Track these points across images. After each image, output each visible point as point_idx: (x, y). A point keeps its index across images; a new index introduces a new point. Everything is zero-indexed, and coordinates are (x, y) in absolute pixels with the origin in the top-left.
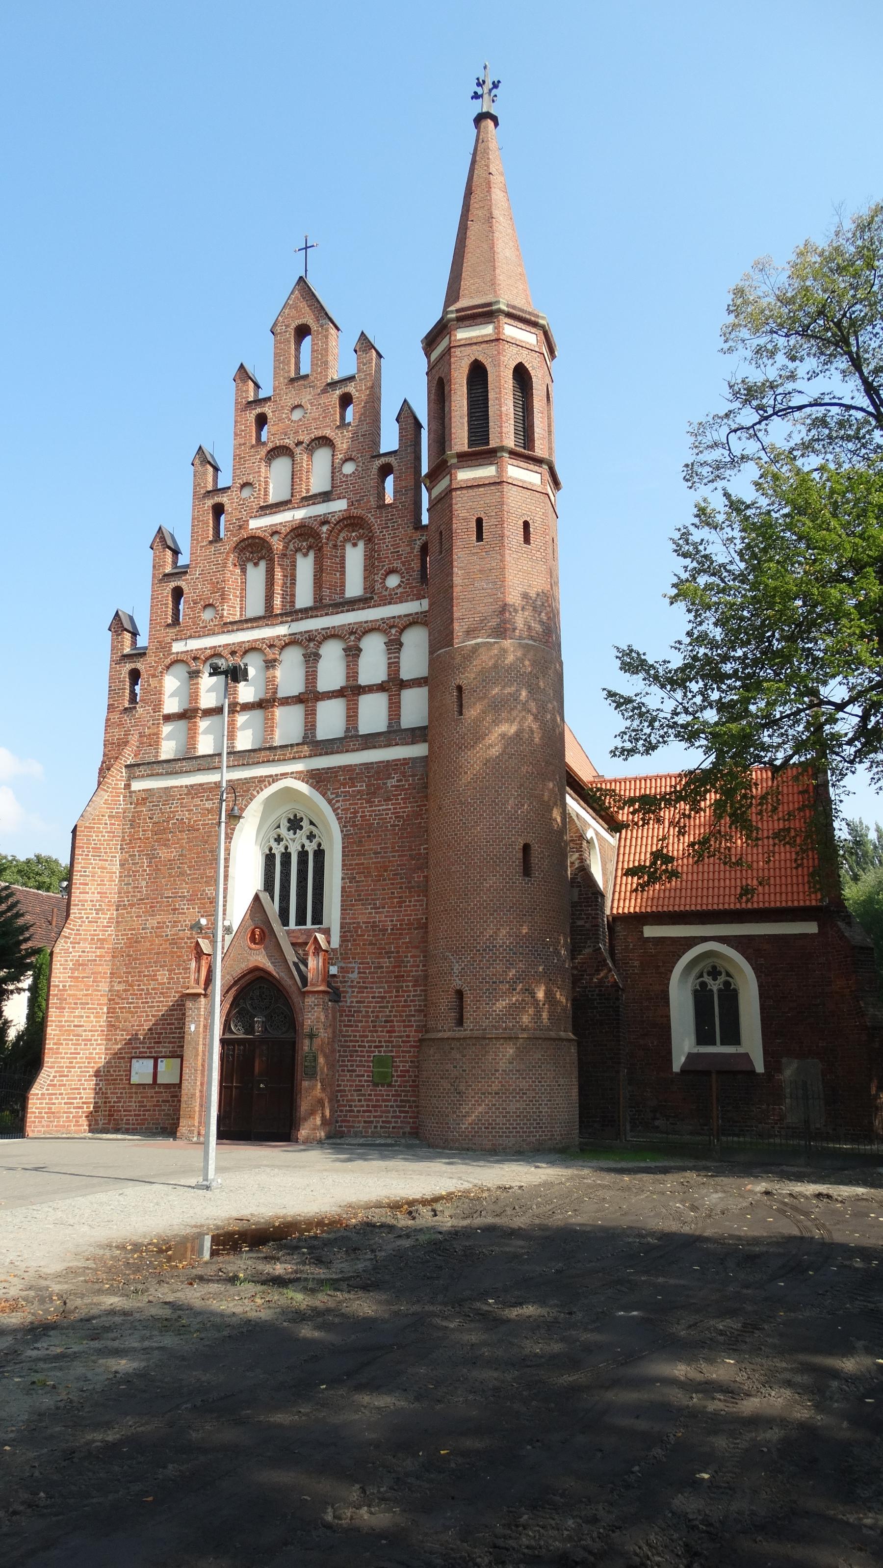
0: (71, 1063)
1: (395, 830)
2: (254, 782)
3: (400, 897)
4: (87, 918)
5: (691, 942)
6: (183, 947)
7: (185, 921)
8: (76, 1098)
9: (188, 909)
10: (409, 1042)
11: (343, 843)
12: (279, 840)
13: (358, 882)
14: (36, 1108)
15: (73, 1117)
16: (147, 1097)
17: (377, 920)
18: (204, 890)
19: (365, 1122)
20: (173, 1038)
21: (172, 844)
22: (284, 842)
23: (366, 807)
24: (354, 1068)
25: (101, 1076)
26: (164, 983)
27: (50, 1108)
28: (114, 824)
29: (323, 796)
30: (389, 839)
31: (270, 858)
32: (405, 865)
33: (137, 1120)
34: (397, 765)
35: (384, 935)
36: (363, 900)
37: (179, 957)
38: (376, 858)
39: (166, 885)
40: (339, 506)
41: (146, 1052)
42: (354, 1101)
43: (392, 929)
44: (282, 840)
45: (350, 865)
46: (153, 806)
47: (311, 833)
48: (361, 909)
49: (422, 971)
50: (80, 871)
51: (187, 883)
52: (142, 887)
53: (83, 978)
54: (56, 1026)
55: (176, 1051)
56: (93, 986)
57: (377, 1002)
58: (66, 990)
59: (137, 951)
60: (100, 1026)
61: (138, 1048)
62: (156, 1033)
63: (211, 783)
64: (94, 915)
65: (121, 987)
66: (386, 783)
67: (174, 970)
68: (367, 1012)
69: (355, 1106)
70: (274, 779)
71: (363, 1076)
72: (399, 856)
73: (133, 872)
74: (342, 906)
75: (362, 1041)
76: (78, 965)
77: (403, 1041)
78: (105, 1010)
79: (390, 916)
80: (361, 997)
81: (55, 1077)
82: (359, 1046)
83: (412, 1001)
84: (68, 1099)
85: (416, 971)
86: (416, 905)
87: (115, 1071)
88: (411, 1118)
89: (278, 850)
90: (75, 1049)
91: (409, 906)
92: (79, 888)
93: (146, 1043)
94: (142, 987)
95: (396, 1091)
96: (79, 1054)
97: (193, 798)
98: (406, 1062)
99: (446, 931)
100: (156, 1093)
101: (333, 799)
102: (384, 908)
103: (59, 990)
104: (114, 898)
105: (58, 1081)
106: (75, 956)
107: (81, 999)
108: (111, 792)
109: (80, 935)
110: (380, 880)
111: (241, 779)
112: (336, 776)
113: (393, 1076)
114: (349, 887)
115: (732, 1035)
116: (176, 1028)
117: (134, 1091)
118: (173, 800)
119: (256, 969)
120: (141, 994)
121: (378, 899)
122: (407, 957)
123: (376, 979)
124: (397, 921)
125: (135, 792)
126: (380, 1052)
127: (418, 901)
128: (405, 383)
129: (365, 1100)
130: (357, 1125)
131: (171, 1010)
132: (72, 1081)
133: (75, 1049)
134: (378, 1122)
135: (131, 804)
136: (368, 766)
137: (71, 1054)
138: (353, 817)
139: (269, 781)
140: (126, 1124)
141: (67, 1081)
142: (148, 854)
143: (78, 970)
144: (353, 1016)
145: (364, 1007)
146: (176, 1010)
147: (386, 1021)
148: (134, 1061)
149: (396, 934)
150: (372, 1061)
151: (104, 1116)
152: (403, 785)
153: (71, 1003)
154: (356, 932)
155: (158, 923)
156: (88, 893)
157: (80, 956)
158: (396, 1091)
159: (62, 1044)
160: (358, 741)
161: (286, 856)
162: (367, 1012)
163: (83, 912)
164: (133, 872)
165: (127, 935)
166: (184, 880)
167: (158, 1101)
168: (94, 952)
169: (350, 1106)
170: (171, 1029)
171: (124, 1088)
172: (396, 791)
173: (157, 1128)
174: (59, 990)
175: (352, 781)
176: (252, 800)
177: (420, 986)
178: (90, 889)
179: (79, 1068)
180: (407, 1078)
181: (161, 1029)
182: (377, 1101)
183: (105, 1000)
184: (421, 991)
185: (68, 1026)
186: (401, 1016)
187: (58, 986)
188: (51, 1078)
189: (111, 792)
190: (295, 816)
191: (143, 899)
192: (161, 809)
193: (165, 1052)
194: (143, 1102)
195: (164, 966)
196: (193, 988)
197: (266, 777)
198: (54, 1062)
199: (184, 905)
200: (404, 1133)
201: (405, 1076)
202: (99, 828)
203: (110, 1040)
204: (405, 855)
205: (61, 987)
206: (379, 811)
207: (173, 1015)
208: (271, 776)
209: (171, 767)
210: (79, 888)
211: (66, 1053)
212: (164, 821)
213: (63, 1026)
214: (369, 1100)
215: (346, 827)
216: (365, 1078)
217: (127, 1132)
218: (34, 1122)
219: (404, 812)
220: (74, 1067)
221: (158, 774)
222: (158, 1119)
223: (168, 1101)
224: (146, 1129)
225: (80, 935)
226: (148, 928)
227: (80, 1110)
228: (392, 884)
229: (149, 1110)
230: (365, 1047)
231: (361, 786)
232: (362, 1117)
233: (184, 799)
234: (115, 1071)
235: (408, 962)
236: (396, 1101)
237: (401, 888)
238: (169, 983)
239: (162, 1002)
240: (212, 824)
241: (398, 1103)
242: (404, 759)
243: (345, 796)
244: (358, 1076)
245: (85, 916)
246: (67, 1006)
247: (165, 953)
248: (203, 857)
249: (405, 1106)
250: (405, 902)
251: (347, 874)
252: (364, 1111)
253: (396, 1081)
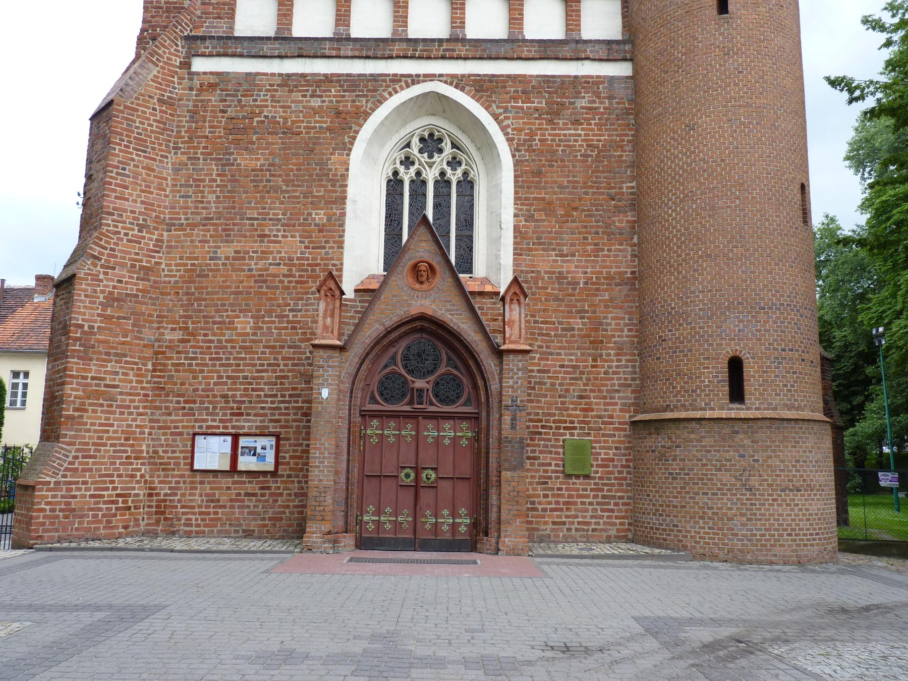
0: (101, 438)
1: (587, 161)
2: (385, 81)
3: (596, 244)
4: (126, 234)
6: (277, 288)
7: (280, 252)
8: (107, 489)
9: (283, 236)
10: (611, 423)
11: (515, 171)
12: (408, 162)
13: (537, 221)
14: (47, 503)
15: (103, 516)
16: (222, 488)
17: (565, 270)
18: (310, 214)
19: (554, 523)
20: (263, 408)
21: (258, 148)
22: (416, 166)
23: (547, 130)
24: (537, 454)
25: (144, 458)
26: (247, 334)
27: (69, 504)
28: (166, 113)
29: (487, 109)
30: (580, 172)
31: (394, 185)
32: (602, 205)
33: (203, 520)
34: (588, 82)
35: (575, 289)
36: (544, 244)
37: (271, 299)
38: (561, 193)
39: (249, 203)
41: (218, 427)
42: (539, 496)
43: (586, 283)
44: (413, 163)
45: (526, 199)
46: (227, 95)
47: (454, 158)
48: (543, 256)
49: (627, 336)
50: (118, 167)
51: (282, 203)
52: (209, 202)
53: (119, 318)
54: (78, 384)
55: (268, 427)
56: (133, 331)
57: (566, 373)
58: (95, 334)
59: (202, 288)
60: (143, 388)
61: (206, 421)
62: (234, 402)
63: (319, 75)
64: (136, 232)
65: (178, 335)
66: (574, 103)
67: (264, 317)
68: (553, 384)
69: (540, 503)
70: (415, 79)
71: (550, 465)
72: (593, 193)
73: (194, 180)
74: (515, 249)
75: (547, 421)
76: (111, 299)
77: (604, 423)
78: (150, 367)
79: (582, 267)
80: (545, 365)
81: (76, 457)
82: (543, 427)
83: (614, 373)
84: (96, 489)
85: (619, 336)
86: (617, 256)
87: (165, 452)
88: (617, 517)
89: (407, 176)
90: (107, 419)
91: (609, 256)
92: (114, 191)
93: (217, 414)
94: (210, 338)
95: (595, 484)
96: (112, 425)
97: (290, 91)
98: (610, 448)
99: (710, 282)
100: (234, 483)
101: (501, 114)
102: (574, 255)
103: (83, 332)
104: (164, 213)
105: (80, 463)
106: (107, 286)
107: (116, 348)
108: (163, 68)
109: (116, 257)
110: (567, 221)
111: (365, 75)
112: (505, 87)
113: (592, 466)
114: (524, 226)
116: (266, 396)
117: (198, 479)
118: (261, 91)
119: (422, 317)
120: (210, 347)
121: (564, 245)
122: (605, 318)
123: (565, 344)
124: (592, 273)
125: (197, 74)
126: (572, 435)
127: (620, 250)
129: (553, 495)
130: (542, 527)
131: (258, 371)
132: (102, 464)
133: (107, 419)
134: (573, 523)
135: (191, 89)
136: (548, 80)
137: (101, 425)
138: (529, 140)
139: (406, 82)
140: (185, 525)
141: (94, 463)
142: (220, 159)
143: (112, 306)
144: (533, 388)
145: (550, 378)
146: (266, 371)
147: (581, 397)
148: (199, 440)
149: (591, 289)
150: (563, 447)
151: (148, 513)
152: (596, 108)
153: (100, 353)
154: (536, 283)
155: (236, 252)
156: (127, 200)
157: (114, 287)
158: (595, 484)
159: (86, 411)
160: (534, 47)
161: (419, 184)
162: (553, 384)
163: (120, 225)
164: (194, 180)
165: (186, 265)
166: (278, 198)
167: (239, 494)
168: (136, 284)
169: (533, 503)
170: (259, 396)
171: (182, 476)
172: (587, 113)
173: (236, 532)
174: (83, 332)
175: (526, 94)
176: (381, 103)
177: (626, 354)
178: (131, 195)
179: (112, 445)
180: (611, 469)
181: (241, 396)
182: (570, 496)
183: (149, 353)
184: (627, 361)
185: (96, 385)
186: (600, 391)
187: (82, 326)
188: (70, 459)
189: (163, 68)
190: (431, 135)
191: (211, 219)
192: (240, 101)
193: (250, 427)
194: (214, 495)
195: (246, 311)
196: (324, 338)
197: (402, 76)
198: (75, 437)
199: (279, 231)
200: (608, 537)
201: (608, 466)
202: (145, 113)
203: (160, 408)
204: (603, 193)
205: (86, 328)
206: (565, 135)
207: (262, 378)
208: (410, 76)
209: (253, 46)
210: (114, 191)
211: (93, 424)
212: (244, 118)
213: (90, 385)
214: (559, 496)
215: (519, 151)
216: (553, 468)
217: (188, 535)
218: (43, 524)
219: (600, 141)
220: (105, 445)
221: (234, 55)
222: (238, 519)
223: (253, 495)
224: (219, 532)
225: (115, 257)
226: (220, 259)
227: (114, 506)
228: (585, 227)
229: (224, 507)
230: (551, 428)
231: (540, 103)
232: (549, 516)
233: (277, 91)
234: (164, 452)
235: (610, 324)
236: (595, 497)
237: (597, 233)
238: (255, 334)
239: (245, 359)
240: (321, 127)
241: (600, 500)
242: (598, 77)
243: (518, 113)
244: (543, 465)
245: (123, 231)
246: (95, 357)
247: (248, 293)
248: (307, 170)
249: (609, 504)
250: (603, 250)
251: (521, 210)
252: (552, 510)
253: (597, 472)
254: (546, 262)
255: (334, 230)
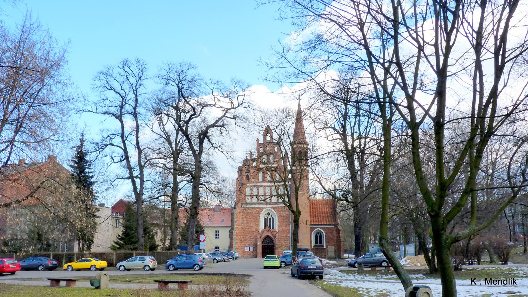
5: (315, 228)
31: (265, 219)
40: (275, 166)
70: (267, 207)
115: (321, 242)
128: (286, 147)
161: (267, 219)
209: (247, 204)
254: (281, 228)
255: (258, 225)
